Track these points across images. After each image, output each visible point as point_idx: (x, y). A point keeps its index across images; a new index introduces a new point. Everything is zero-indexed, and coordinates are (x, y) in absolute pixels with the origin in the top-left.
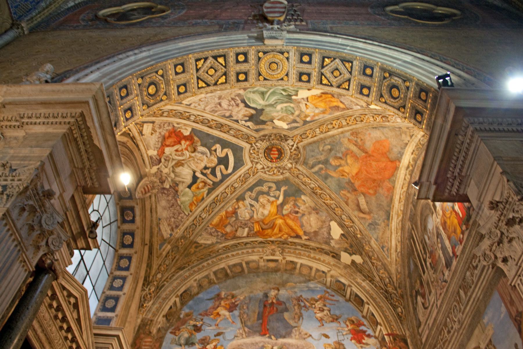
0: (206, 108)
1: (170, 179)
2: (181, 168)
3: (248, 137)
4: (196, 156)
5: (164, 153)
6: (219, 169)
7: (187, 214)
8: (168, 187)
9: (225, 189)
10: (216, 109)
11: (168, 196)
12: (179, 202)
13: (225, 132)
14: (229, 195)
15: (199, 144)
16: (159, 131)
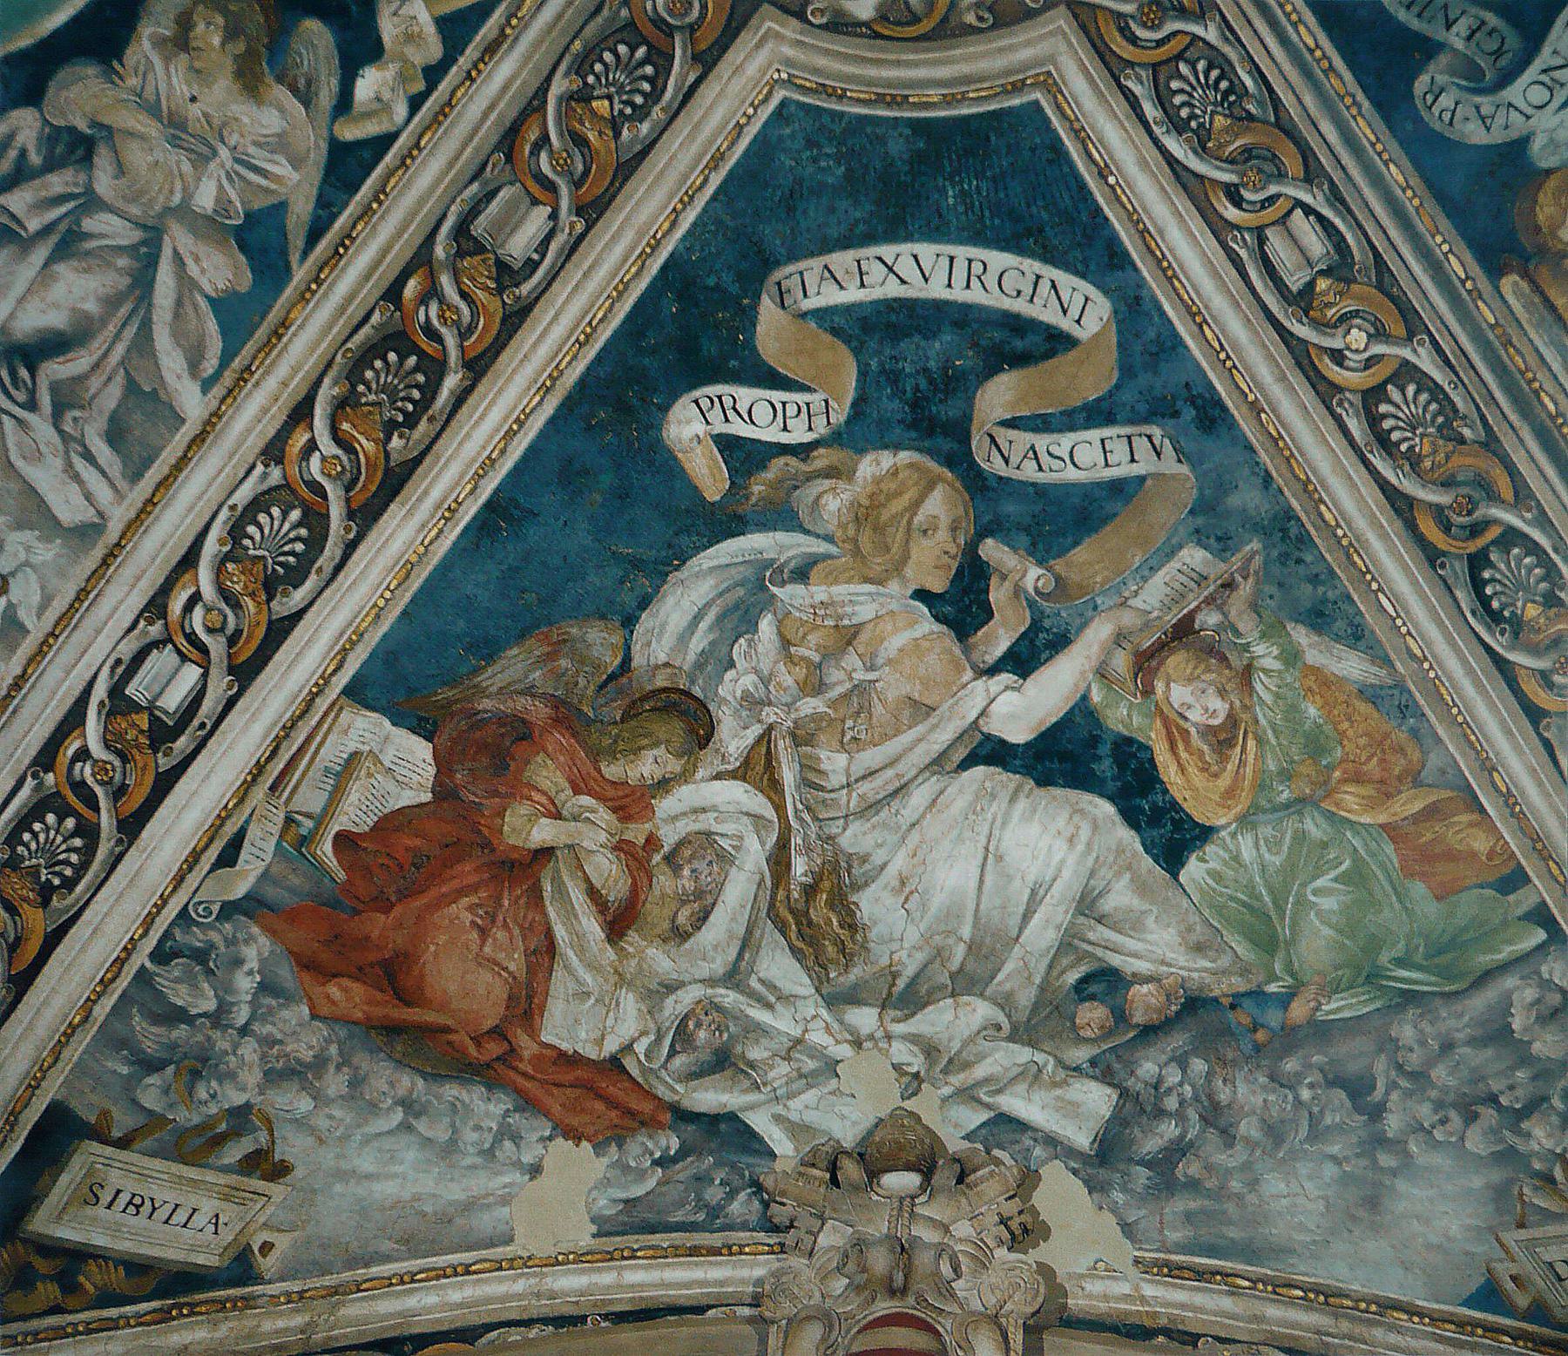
0: (68, 507)
1: (1007, 1057)
2: (873, 904)
3: (630, 32)
4: (752, 703)
5: (614, 1064)
6: (1024, 439)
7: (1541, 935)
8: (1097, 1099)
9: (1326, 391)
10: (112, 397)
11: (1216, 1116)
12: (1337, 1007)
13: (515, 319)
14: (1425, 361)
15: (600, 641)
16: (252, 1077)
